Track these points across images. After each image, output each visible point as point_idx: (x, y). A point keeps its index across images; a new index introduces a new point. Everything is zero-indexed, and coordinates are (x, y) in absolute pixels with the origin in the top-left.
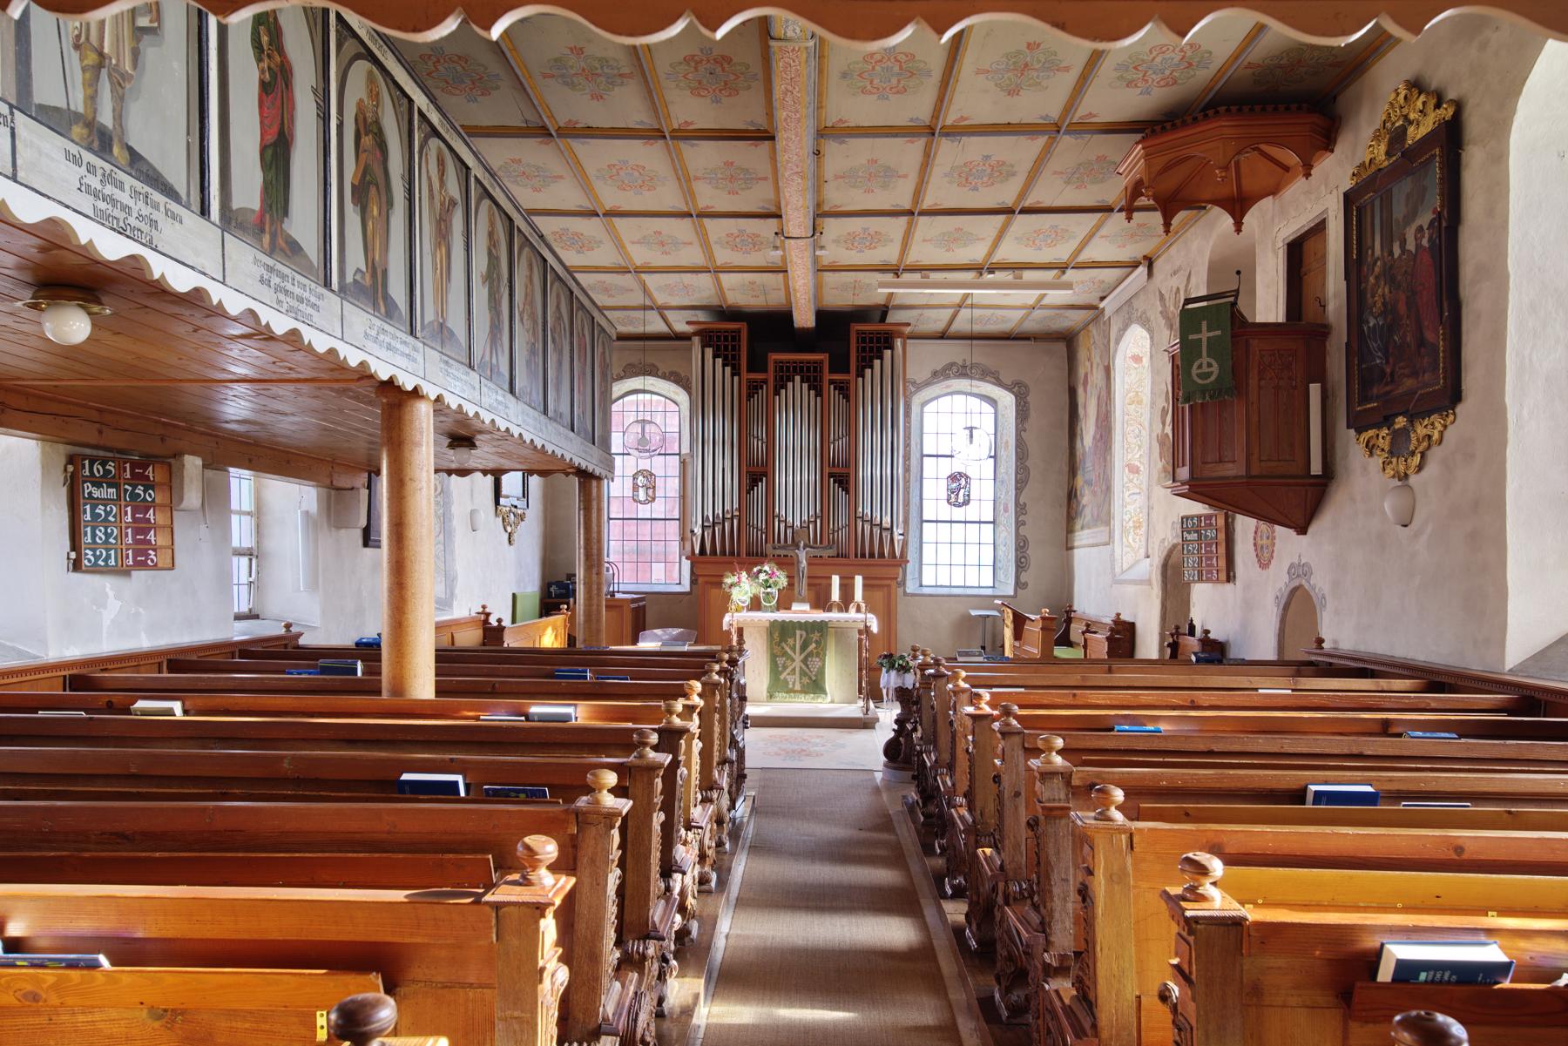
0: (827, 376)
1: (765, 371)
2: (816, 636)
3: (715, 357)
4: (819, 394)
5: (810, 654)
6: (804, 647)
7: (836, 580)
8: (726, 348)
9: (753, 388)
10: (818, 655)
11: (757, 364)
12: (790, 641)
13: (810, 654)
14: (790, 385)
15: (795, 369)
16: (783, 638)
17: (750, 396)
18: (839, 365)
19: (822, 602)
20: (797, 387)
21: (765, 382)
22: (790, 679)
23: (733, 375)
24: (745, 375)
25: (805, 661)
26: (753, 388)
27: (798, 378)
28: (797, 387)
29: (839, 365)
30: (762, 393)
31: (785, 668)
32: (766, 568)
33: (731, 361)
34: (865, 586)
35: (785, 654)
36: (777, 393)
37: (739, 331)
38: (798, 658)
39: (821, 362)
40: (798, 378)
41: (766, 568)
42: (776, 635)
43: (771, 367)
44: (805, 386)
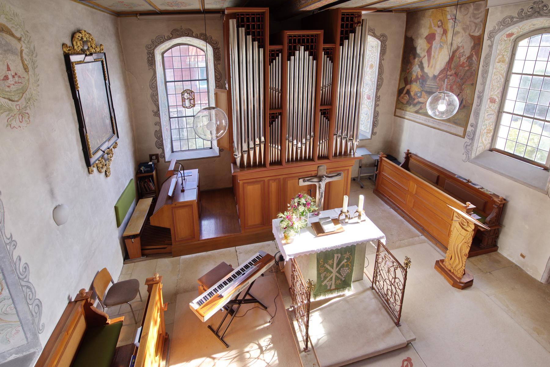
0: (322, 46)
1: (280, 43)
2: (347, 256)
3: (247, 34)
4: (316, 58)
5: (343, 266)
8: (254, 28)
10: (347, 266)
11: (276, 39)
12: (330, 262)
13: (343, 266)
14: (297, 53)
15: (299, 40)
16: (326, 261)
17: (271, 62)
20: (301, 54)
21: (281, 51)
23: (259, 47)
24: (269, 47)
25: (338, 272)
28: (301, 54)
30: (279, 59)
35: (327, 270)
36: (289, 59)
37: (263, 14)
38: (334, 271)
39: (317, 35)
43: (286, 41)
44: (307, 53)
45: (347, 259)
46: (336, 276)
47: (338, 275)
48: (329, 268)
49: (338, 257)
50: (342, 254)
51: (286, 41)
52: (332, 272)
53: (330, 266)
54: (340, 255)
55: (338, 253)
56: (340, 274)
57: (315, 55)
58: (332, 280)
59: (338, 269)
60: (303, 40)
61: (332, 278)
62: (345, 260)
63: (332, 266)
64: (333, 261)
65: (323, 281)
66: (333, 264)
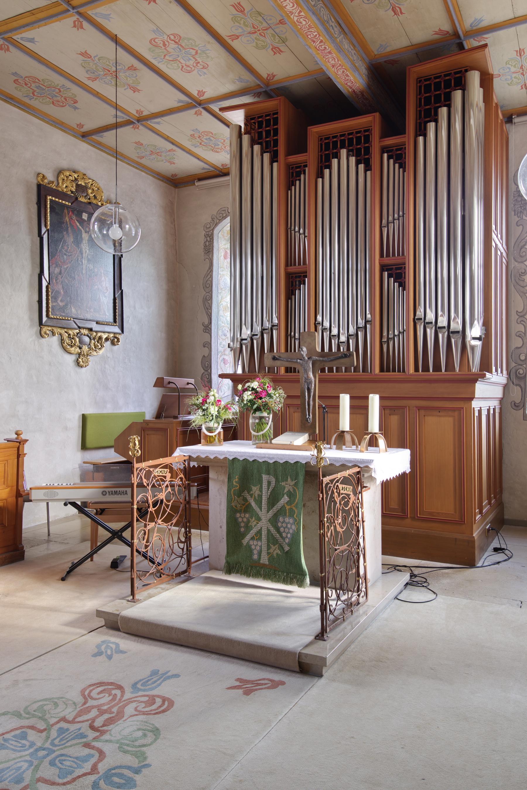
2: (288, 485)
5: (281, 512)
6: (273, 500)
7: (345, 400)
9: (293, 175)
13: (281, 512)
14: (335, 161)
18: (393, 126)
19: (322, 431)
20: (345, 162)
22: (256, 546)
25: (274, 521)
26: (293, 175)
27: (344, 153)
28: (345, 162)
29: (393, 126)
31: (248, 528)
32: (255, 384)
33: (270, 147)
34: (382, 408)
35: (247, 508)
36: (320, 175)
40: (344, 153)
41: (255, 384)
42: (236, 480)
43: (313, 145)
44: (353, 160)
45: (291, 495)
46: (269, 531)
47: (272, 529)
48: (253, 504)
49: (269, 483)
50: (277, 481)
51: (313, 145)
52: (259, 519)
53: (255, 500)
54: (273, 480)
55: (268, 473)
56: (278, 530)
57: (364, 158)
58: (260, 539)
59: (271, 513)
60: (351, 141)
61: (259, 532)
62: (286, 498)
63: (259, 502)
64: (261, 491)
65: (244, 535)
66: (260, 496)
